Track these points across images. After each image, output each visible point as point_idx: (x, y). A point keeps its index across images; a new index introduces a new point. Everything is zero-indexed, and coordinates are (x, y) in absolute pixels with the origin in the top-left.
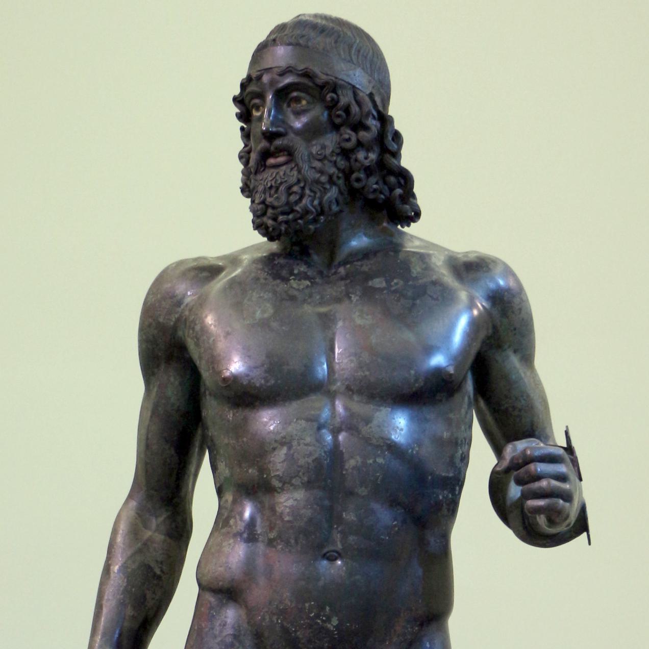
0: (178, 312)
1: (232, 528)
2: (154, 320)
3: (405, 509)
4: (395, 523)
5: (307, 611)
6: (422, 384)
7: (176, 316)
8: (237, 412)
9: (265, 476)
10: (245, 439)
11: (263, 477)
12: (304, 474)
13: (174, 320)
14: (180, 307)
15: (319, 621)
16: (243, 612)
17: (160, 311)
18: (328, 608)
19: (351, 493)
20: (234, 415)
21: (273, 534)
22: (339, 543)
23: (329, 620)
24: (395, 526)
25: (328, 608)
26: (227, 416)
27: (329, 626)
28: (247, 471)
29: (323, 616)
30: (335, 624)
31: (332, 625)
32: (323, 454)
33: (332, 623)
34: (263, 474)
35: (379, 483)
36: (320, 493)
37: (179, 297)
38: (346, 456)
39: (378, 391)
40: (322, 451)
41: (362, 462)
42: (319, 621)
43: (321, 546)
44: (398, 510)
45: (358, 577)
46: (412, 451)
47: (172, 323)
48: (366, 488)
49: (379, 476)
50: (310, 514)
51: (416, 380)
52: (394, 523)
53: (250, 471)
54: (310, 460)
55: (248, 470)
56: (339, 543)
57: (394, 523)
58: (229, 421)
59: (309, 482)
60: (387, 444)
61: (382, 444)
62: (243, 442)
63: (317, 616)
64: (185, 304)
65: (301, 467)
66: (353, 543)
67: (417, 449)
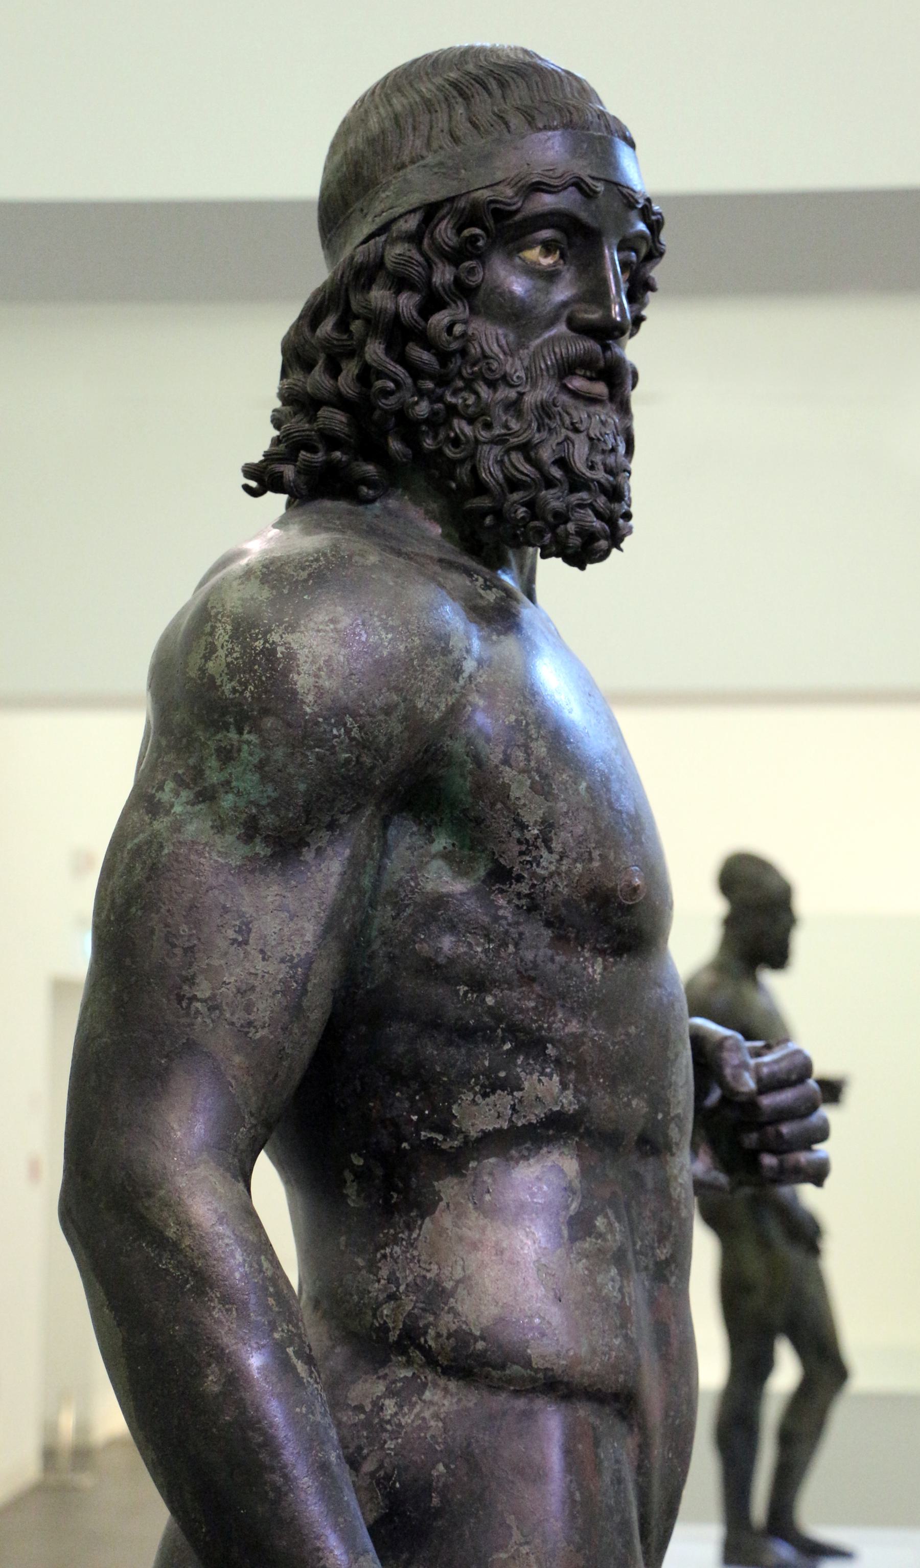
0: (454, 691)
1: (605, 1240)
2: (405, 700)
7: (451, 700)
8: (615, 964)
9: (660, 1116)
10: (632, 1030)
11: (655, 1118)
13: (443, 707)
14: (457, 680)
16: (631, 1443)
17: (422, 680)
20: (605, 968)
21: (665, 1251)
26: (585, 968)
28: (628, 1104)
34: (656, 1113)
37: (456, 655)
47: (437, 716)
53: (634, 1103)
55: (629, 1100)
58: (592, 981)
62: (628, 1034)
64: (466, 675)
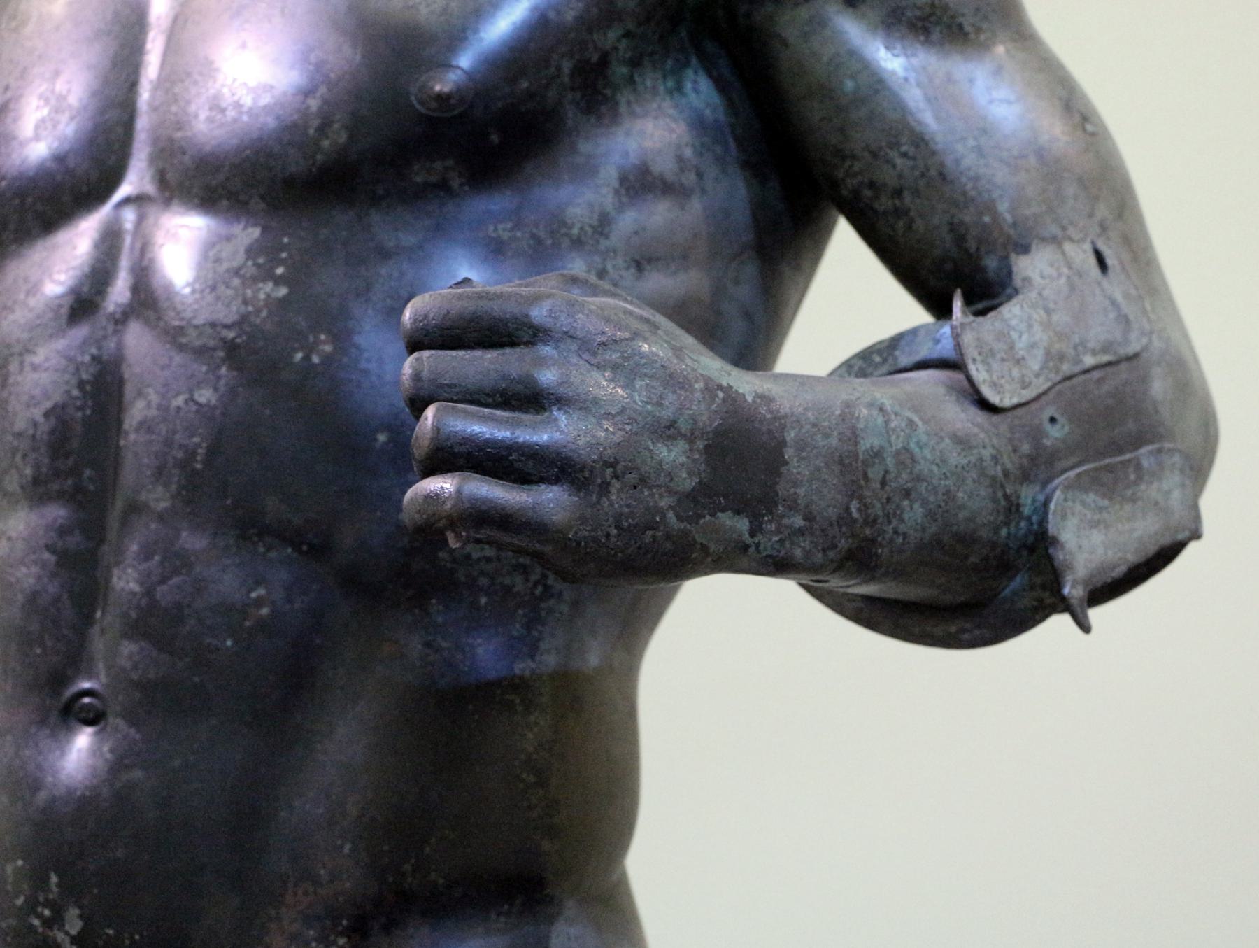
3: (297, 547)
4: (261, 591)
5: (9, 887)
6: (343, 138)
12: (24, 456)
15: (36, 922)
18: (54, 879)
19: (134, 508)
22: (101, 665)
23: (56, 920)
24: (259, 603)
25: (54, 879)
27: (60, 936)
29: (45, 906)
30: (73, 932)
31: (67, 933)
32: (76, 393)
33: (67, 927)
35: (199, 466)
36: (57, 513)
38: (129, 390)
39: (221, 177)
40: (74, 381)
41: (159, 407)
42: (36, 922)
43: (58, 680)
44: (269, 549)
45: (137, 774)
46: (307, 358)
48: (166, 485)
49: (198, 445)
50: (32, 581)
51: (323, 129)
52: (254, 595)
54: (37, 413)
56: (101, 665)
57: (254, 595)
59: (36, 481)
60: (223, 340)
61: (212, 343)
63: (31, 907)
65: (19, 435)
66: (128, 665)
67: (328, 348)
